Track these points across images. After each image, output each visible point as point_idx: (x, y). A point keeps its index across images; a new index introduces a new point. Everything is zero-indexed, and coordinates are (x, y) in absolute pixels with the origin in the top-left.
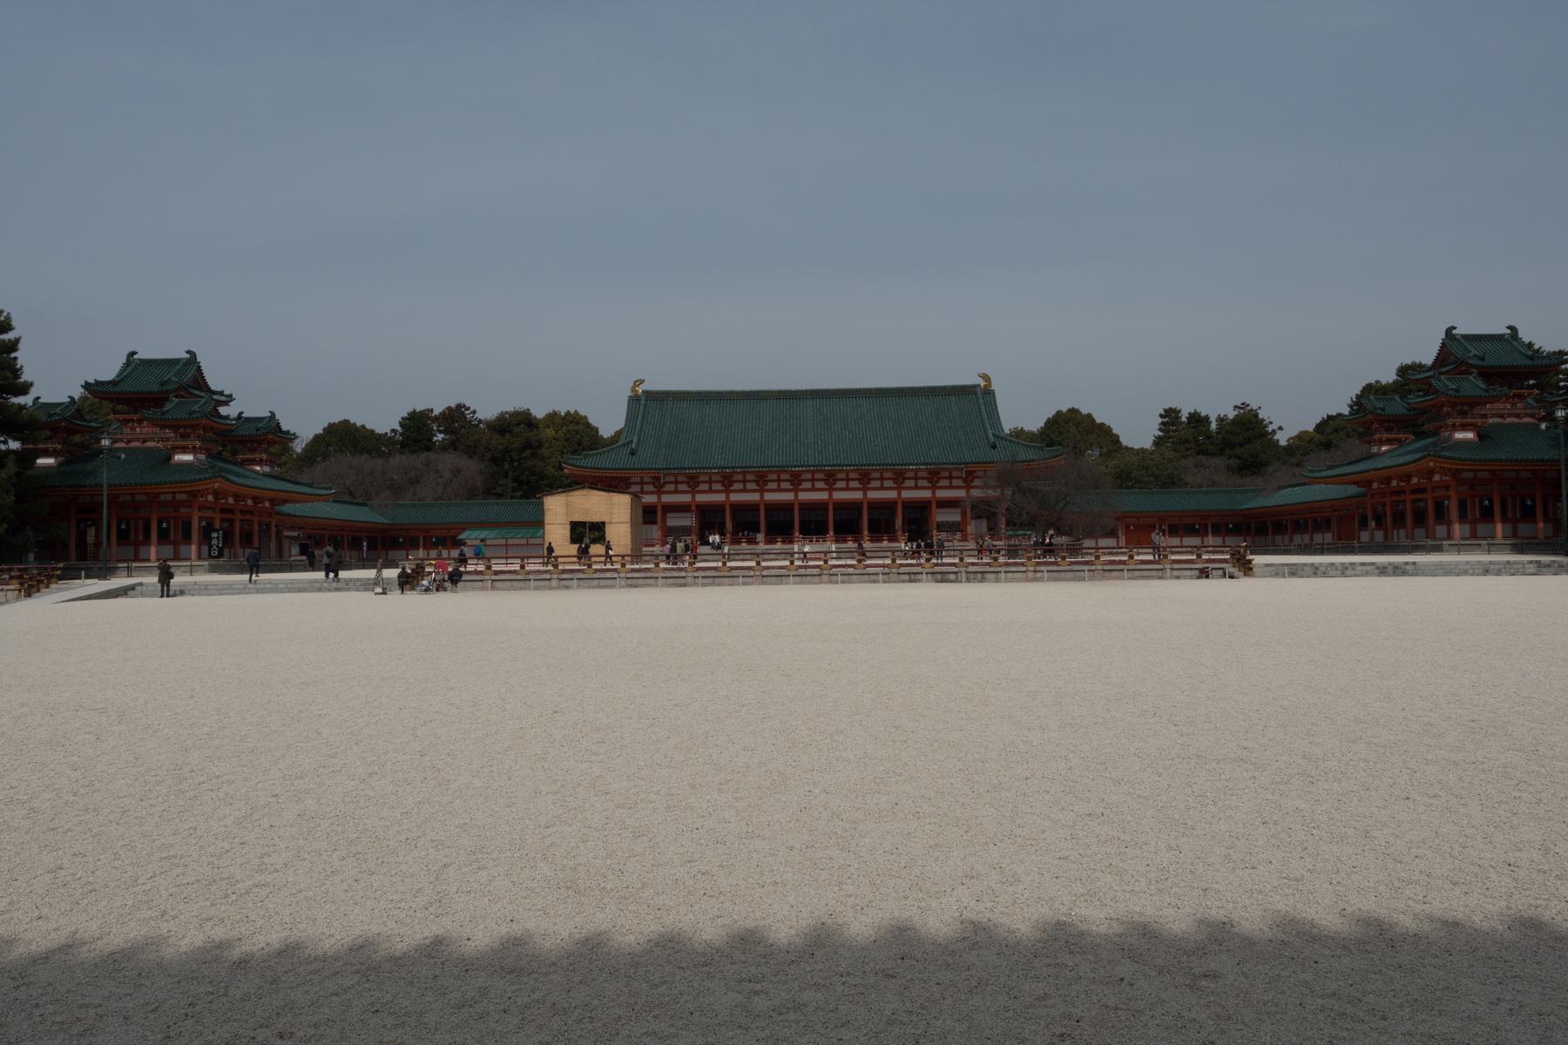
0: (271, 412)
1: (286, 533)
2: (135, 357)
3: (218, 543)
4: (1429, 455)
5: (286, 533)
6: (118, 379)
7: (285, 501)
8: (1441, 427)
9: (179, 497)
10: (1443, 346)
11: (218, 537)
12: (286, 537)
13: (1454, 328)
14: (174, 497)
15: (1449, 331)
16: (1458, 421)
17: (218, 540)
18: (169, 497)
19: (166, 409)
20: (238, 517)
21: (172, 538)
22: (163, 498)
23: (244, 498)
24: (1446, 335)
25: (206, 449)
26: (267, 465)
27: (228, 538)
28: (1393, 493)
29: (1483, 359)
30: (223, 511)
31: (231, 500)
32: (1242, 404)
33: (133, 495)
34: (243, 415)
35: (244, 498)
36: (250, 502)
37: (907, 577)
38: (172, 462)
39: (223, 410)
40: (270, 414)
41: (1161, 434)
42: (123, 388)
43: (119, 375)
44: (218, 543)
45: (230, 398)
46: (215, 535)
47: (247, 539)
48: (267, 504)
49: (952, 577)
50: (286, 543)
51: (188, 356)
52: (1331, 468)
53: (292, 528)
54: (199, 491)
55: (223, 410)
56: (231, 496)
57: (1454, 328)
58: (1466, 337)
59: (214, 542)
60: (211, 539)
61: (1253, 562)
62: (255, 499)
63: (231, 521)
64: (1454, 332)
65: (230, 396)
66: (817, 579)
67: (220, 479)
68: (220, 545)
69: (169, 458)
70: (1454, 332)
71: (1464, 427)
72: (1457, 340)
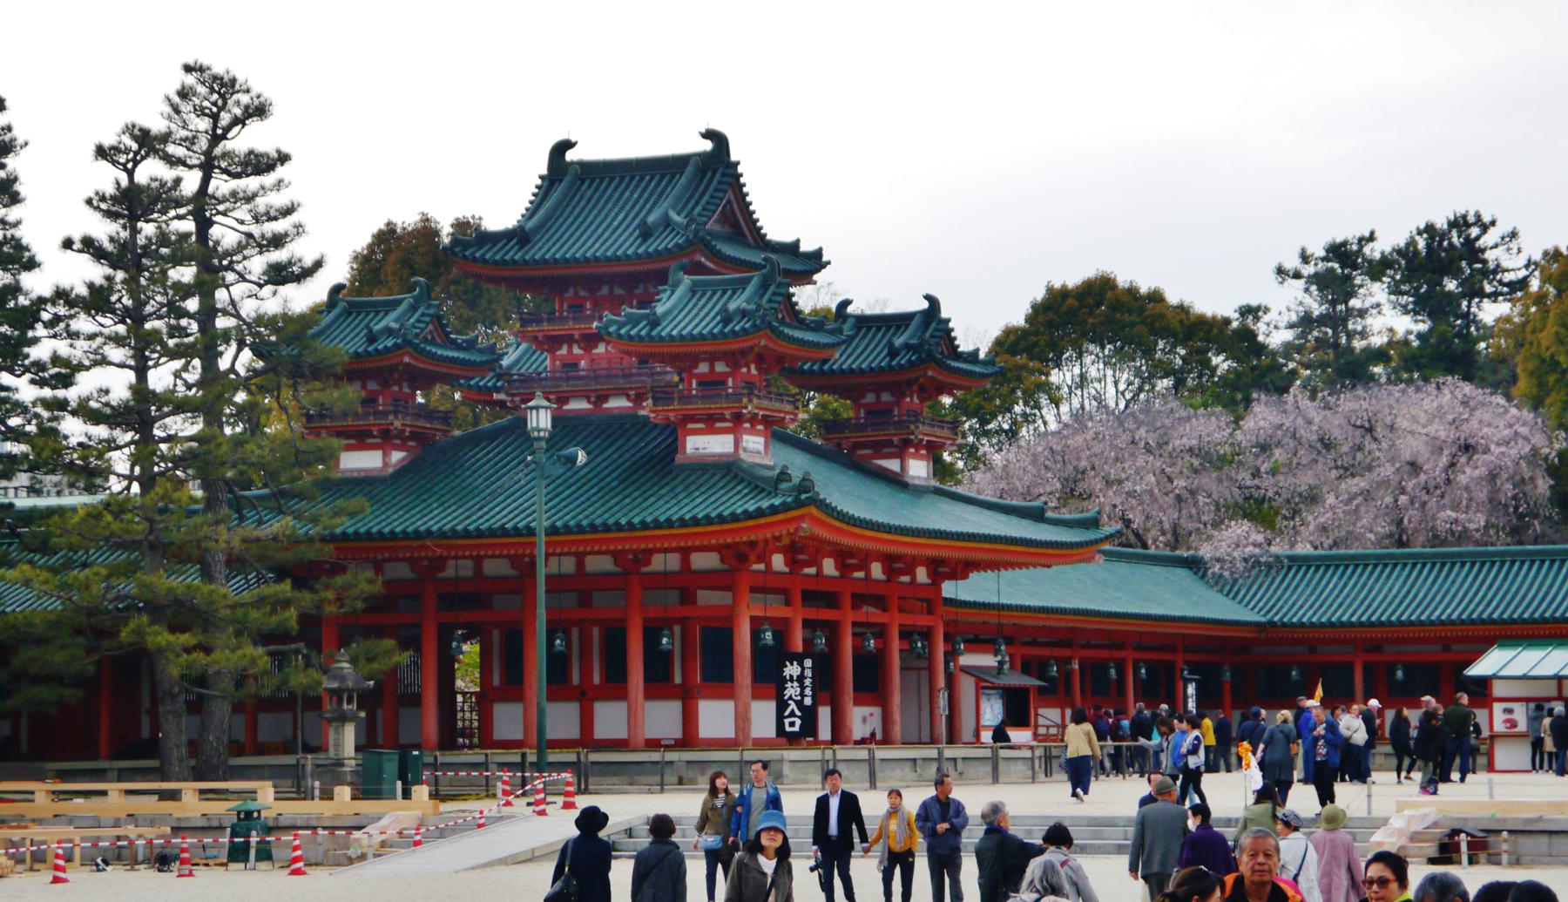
0: (928, 297)
1: (966, 660)
2: (571, 156)
3: (802, 695)
5: (966, 660)
6: (530, 225)
7: (961, 570)
9: (704, 561)
11: (801, 679)
12: (966, 670)
14: (685, 562)
17: (802, 687)
18: (672, 562)
19: (660, 309)
20: (847, 618)
21: (678, 679)
22: (658, 563)
23: (865, 559)
25: (767, 421)
26: (917, 456)
27: (826, 685)
30: (809, 597)
31: (829, 567)
33: (580, 558)
34: (850, 309)
35: (865, 559)
36: (877, 570)
38: (679, 459)
39: (807, 298)
40: (925, 305)
42: (537, 252)
43: (531, 213)
44: (802, 695)
45: (815, 261)
46: (792, 670)
47: (872, 686)
48: (922, 575)
50: (967, 686)
51: (707, 146)
53: (979, 642)
54: (752, 544)
55: (807, 298)
56: (778, 550)
59: (792, 690)
60: (781, 683)
62: (888, 560)
63: (832, 630)
65: (818, 254)
67: (813, 510)
68: (808, 701)
69: (674, 446)
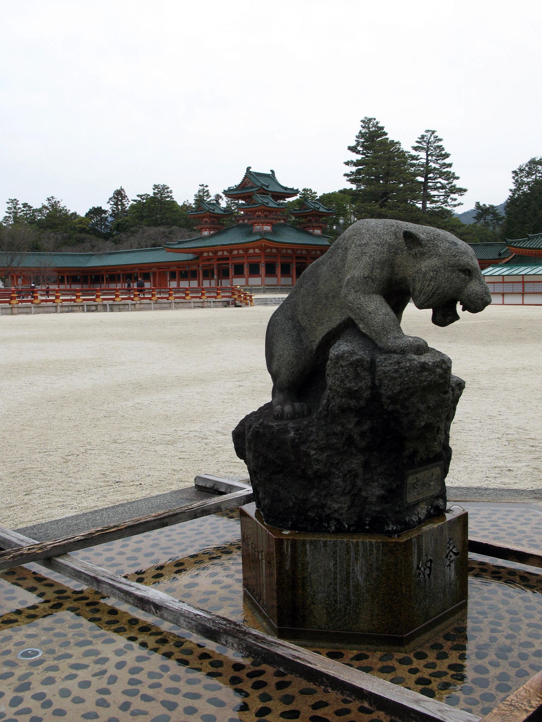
4: (263, 239)
8: (254, 223)
10: (246, 177)
13: (250, 168)
15: (248, 169)
16: (267, 221)
24: (247, 171)
28: (219, 259)
29: (268, 187)
32: (52, 197)
37: (67, 309)
41: (8, 215)
49: (93, 308)
52: (180, 243)
57: (250, 168)
58: (255, 173)
61: (253, 297)
64: (251, 170)
66: (9, 311)
70: (251, 170)
71: (267, 224)
72: (252, 175)
